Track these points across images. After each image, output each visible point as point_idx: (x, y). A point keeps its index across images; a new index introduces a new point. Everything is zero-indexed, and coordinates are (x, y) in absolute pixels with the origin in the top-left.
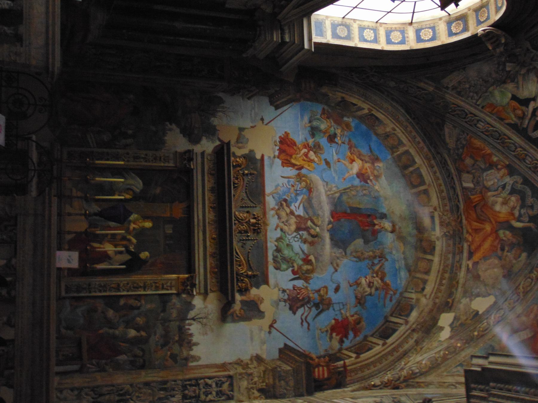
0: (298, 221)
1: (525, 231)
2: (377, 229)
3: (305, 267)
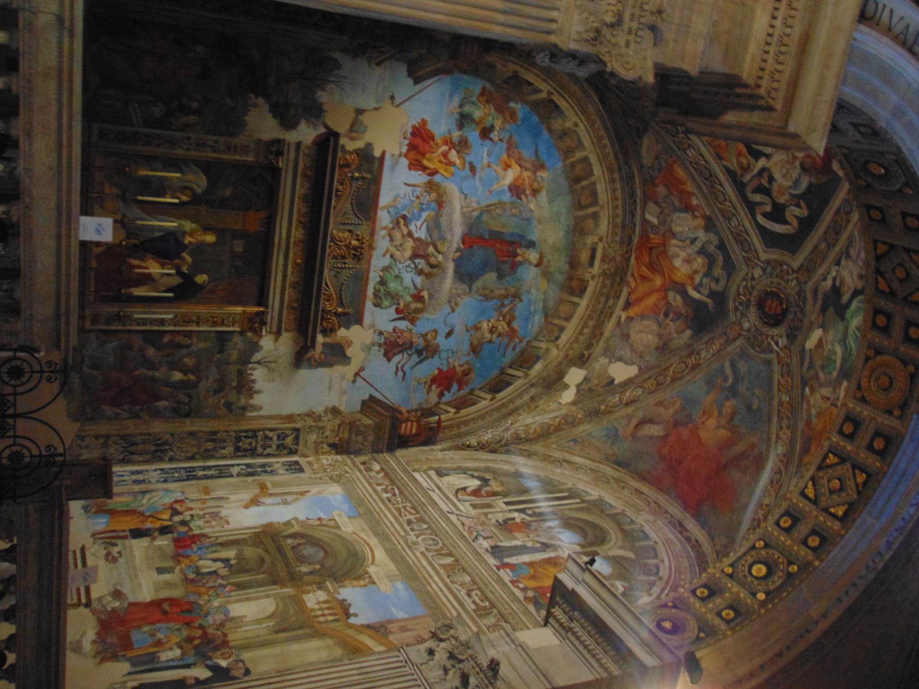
1: (698, 306)
3: (414, 306)
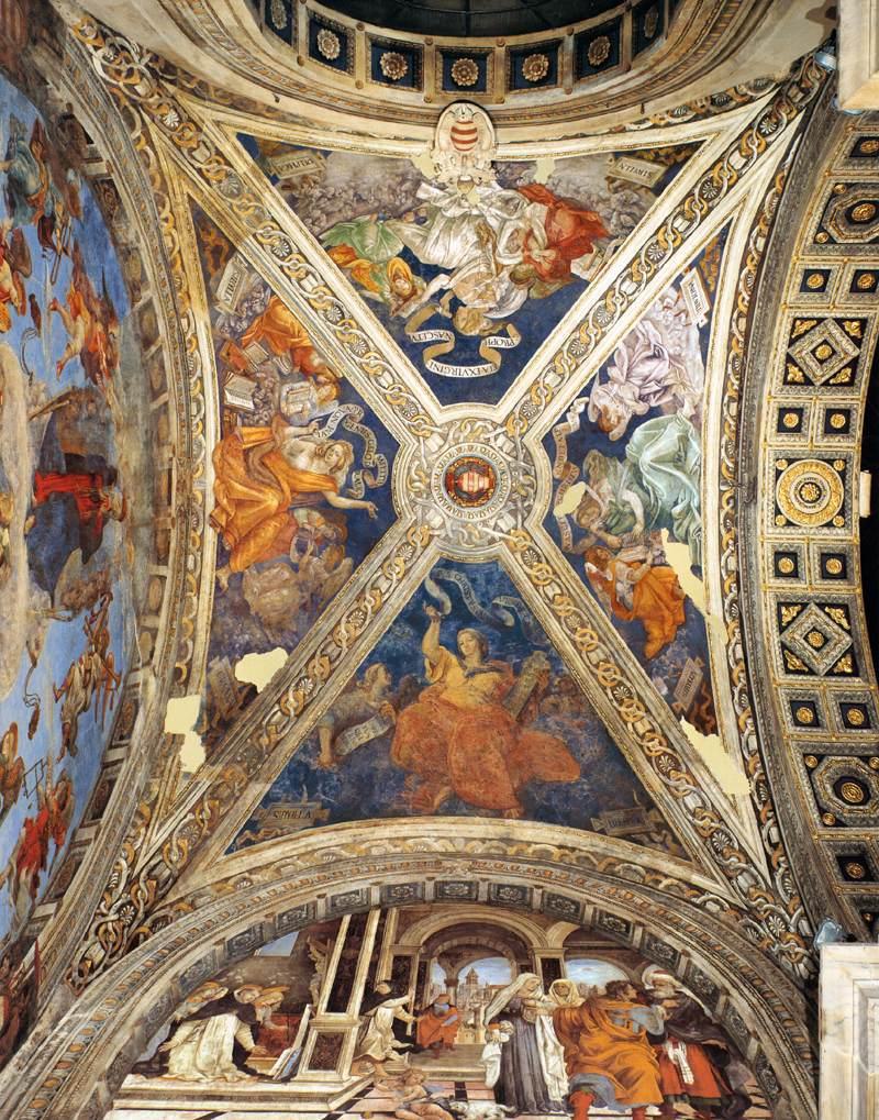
1: (353, 516)
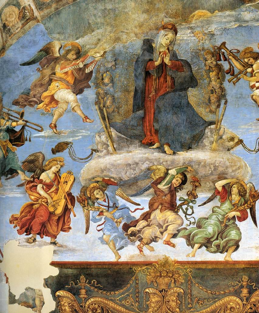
0: (160, 207)
2: (170, 60)
3: (235, 197)
